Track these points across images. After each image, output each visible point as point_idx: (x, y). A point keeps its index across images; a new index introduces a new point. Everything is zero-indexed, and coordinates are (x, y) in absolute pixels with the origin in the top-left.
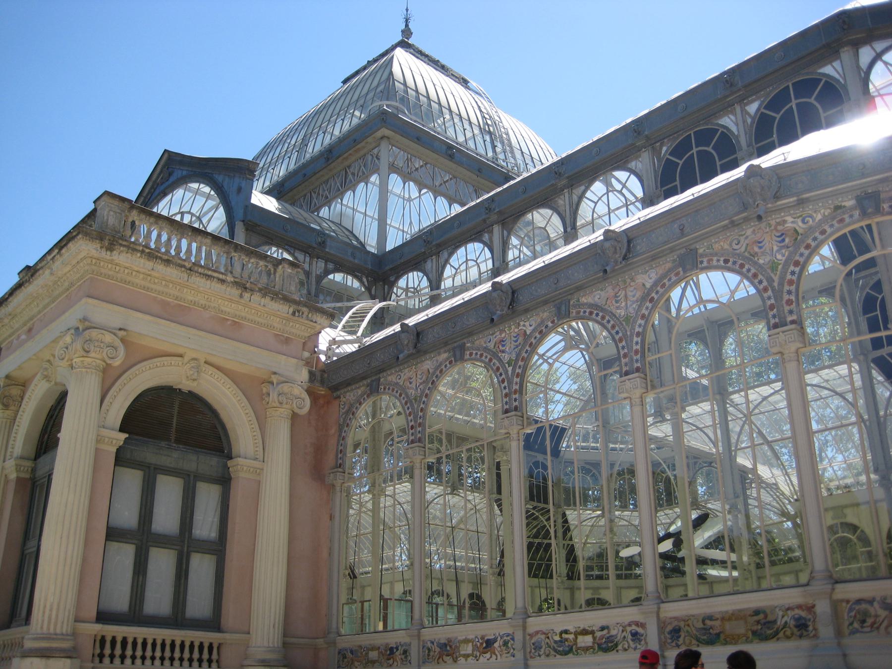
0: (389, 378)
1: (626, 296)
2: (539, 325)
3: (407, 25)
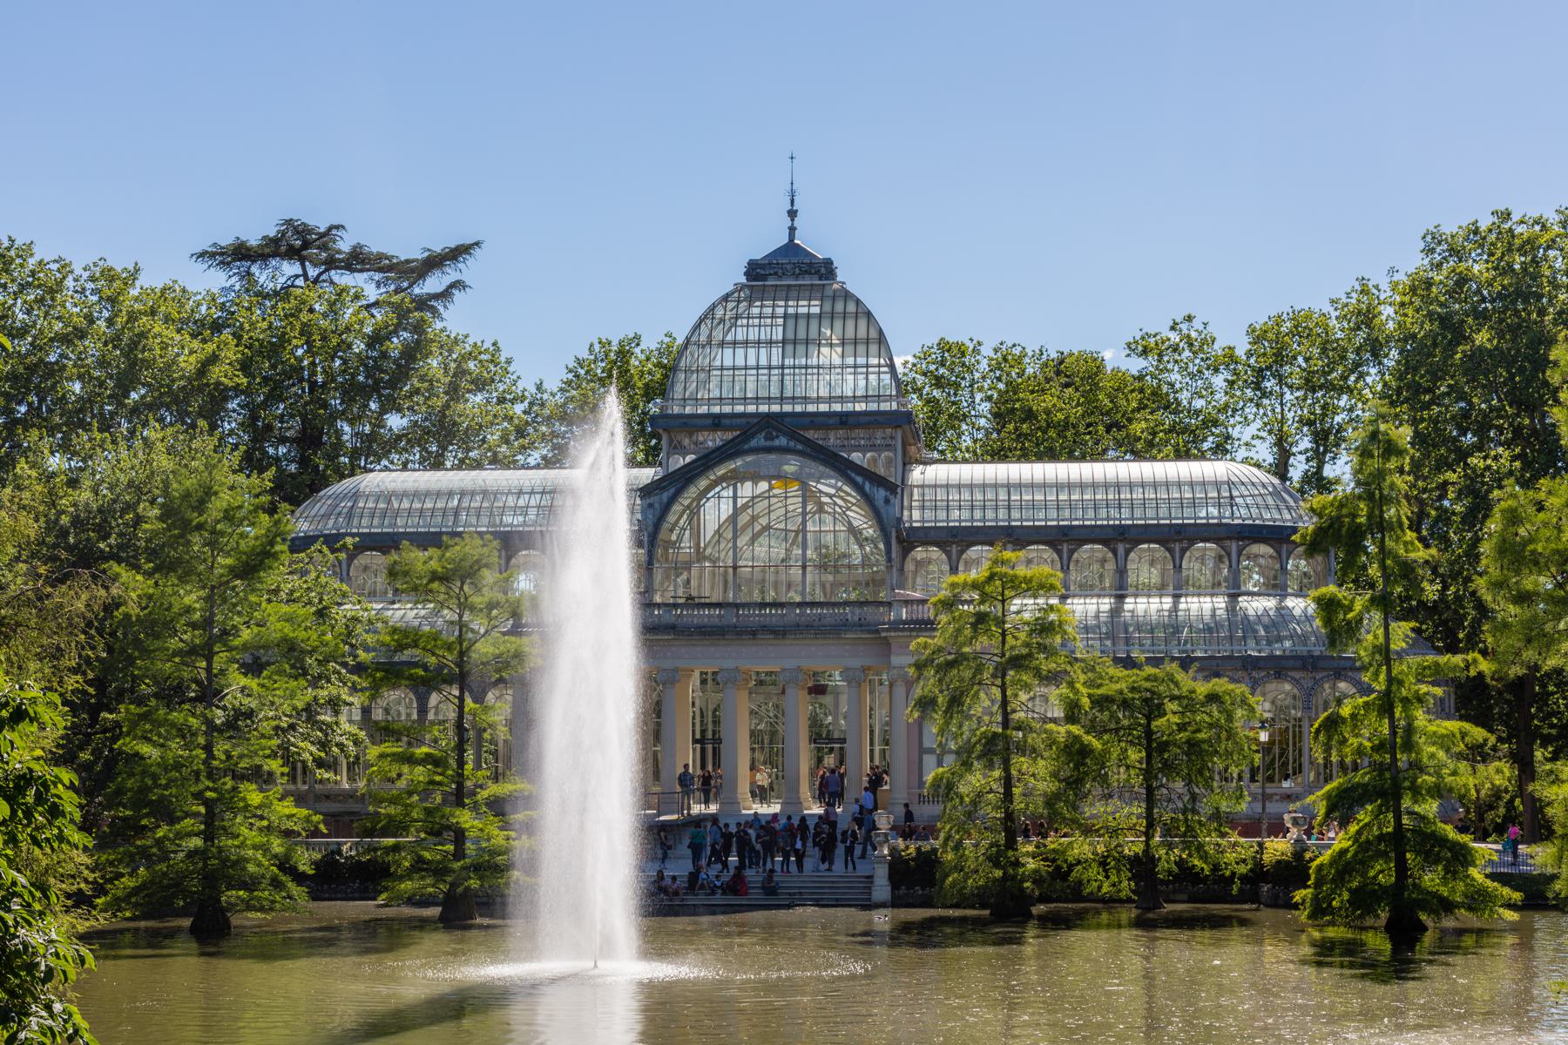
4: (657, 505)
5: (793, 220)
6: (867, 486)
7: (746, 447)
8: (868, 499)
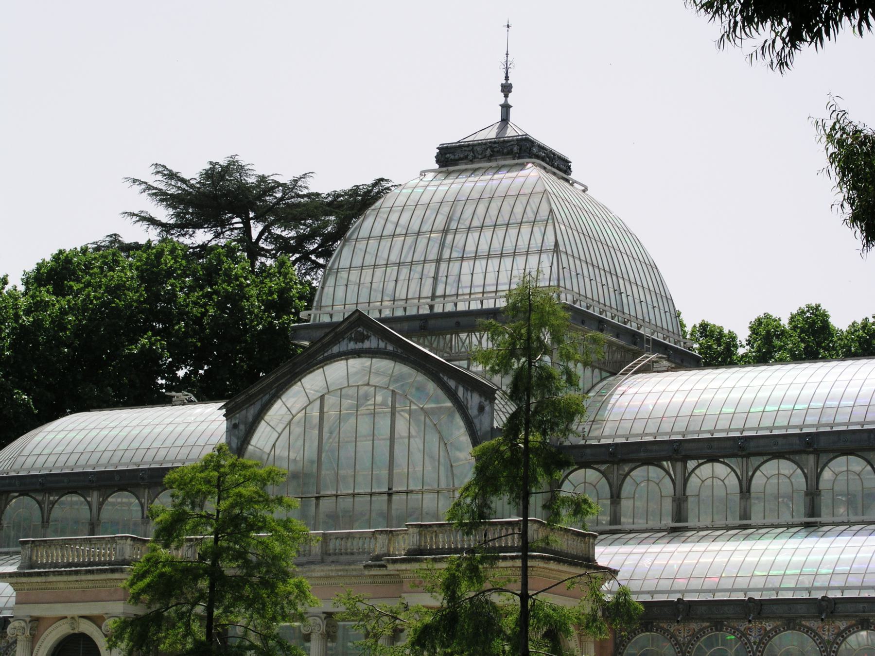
0: (661, 625)
1: (829, 630)
2: (775, 627)
3: (507, 78)
4: (242, 427)
5: (506, 96)
6: (461, 392)
7: (335, 349)
8: (461, 408)
